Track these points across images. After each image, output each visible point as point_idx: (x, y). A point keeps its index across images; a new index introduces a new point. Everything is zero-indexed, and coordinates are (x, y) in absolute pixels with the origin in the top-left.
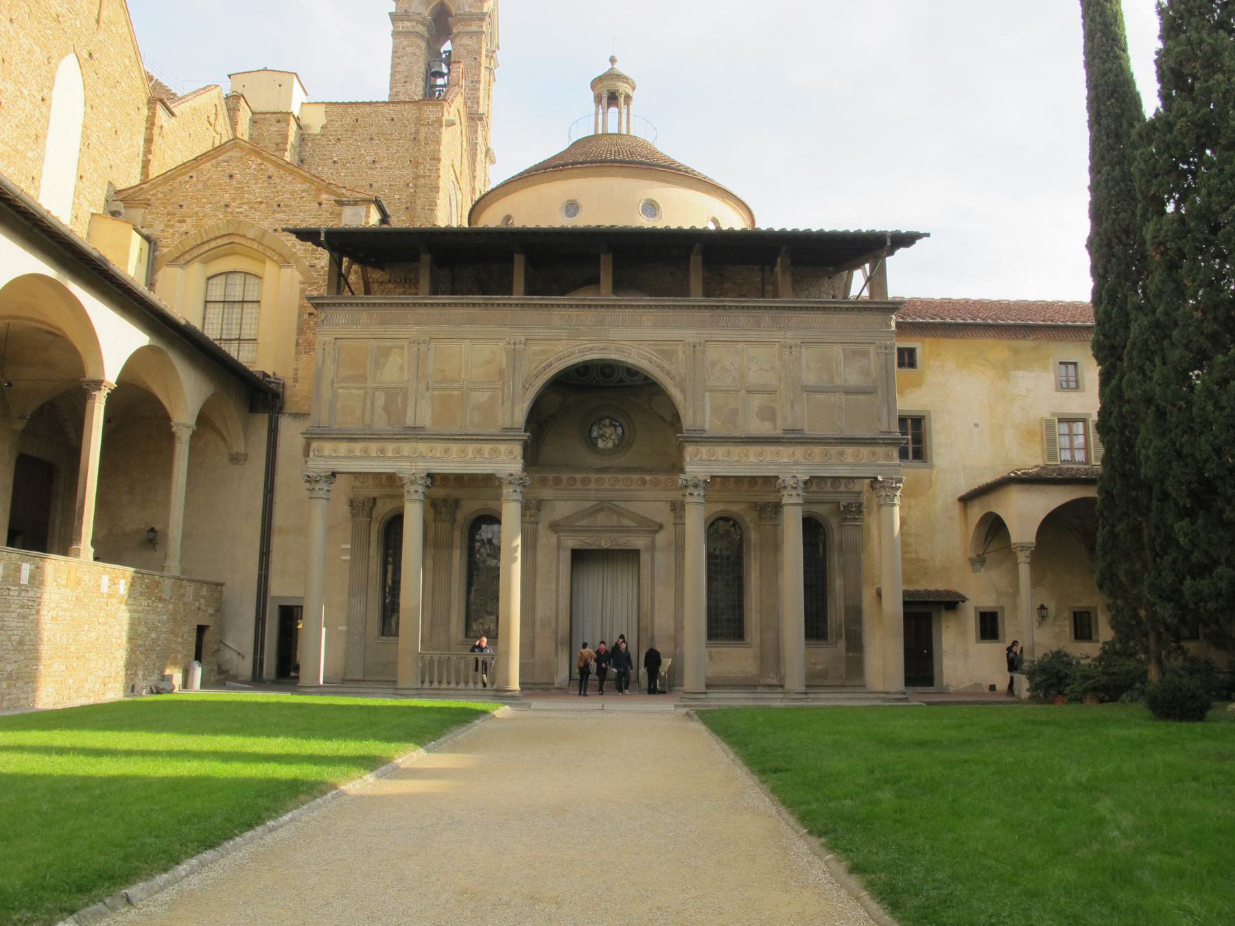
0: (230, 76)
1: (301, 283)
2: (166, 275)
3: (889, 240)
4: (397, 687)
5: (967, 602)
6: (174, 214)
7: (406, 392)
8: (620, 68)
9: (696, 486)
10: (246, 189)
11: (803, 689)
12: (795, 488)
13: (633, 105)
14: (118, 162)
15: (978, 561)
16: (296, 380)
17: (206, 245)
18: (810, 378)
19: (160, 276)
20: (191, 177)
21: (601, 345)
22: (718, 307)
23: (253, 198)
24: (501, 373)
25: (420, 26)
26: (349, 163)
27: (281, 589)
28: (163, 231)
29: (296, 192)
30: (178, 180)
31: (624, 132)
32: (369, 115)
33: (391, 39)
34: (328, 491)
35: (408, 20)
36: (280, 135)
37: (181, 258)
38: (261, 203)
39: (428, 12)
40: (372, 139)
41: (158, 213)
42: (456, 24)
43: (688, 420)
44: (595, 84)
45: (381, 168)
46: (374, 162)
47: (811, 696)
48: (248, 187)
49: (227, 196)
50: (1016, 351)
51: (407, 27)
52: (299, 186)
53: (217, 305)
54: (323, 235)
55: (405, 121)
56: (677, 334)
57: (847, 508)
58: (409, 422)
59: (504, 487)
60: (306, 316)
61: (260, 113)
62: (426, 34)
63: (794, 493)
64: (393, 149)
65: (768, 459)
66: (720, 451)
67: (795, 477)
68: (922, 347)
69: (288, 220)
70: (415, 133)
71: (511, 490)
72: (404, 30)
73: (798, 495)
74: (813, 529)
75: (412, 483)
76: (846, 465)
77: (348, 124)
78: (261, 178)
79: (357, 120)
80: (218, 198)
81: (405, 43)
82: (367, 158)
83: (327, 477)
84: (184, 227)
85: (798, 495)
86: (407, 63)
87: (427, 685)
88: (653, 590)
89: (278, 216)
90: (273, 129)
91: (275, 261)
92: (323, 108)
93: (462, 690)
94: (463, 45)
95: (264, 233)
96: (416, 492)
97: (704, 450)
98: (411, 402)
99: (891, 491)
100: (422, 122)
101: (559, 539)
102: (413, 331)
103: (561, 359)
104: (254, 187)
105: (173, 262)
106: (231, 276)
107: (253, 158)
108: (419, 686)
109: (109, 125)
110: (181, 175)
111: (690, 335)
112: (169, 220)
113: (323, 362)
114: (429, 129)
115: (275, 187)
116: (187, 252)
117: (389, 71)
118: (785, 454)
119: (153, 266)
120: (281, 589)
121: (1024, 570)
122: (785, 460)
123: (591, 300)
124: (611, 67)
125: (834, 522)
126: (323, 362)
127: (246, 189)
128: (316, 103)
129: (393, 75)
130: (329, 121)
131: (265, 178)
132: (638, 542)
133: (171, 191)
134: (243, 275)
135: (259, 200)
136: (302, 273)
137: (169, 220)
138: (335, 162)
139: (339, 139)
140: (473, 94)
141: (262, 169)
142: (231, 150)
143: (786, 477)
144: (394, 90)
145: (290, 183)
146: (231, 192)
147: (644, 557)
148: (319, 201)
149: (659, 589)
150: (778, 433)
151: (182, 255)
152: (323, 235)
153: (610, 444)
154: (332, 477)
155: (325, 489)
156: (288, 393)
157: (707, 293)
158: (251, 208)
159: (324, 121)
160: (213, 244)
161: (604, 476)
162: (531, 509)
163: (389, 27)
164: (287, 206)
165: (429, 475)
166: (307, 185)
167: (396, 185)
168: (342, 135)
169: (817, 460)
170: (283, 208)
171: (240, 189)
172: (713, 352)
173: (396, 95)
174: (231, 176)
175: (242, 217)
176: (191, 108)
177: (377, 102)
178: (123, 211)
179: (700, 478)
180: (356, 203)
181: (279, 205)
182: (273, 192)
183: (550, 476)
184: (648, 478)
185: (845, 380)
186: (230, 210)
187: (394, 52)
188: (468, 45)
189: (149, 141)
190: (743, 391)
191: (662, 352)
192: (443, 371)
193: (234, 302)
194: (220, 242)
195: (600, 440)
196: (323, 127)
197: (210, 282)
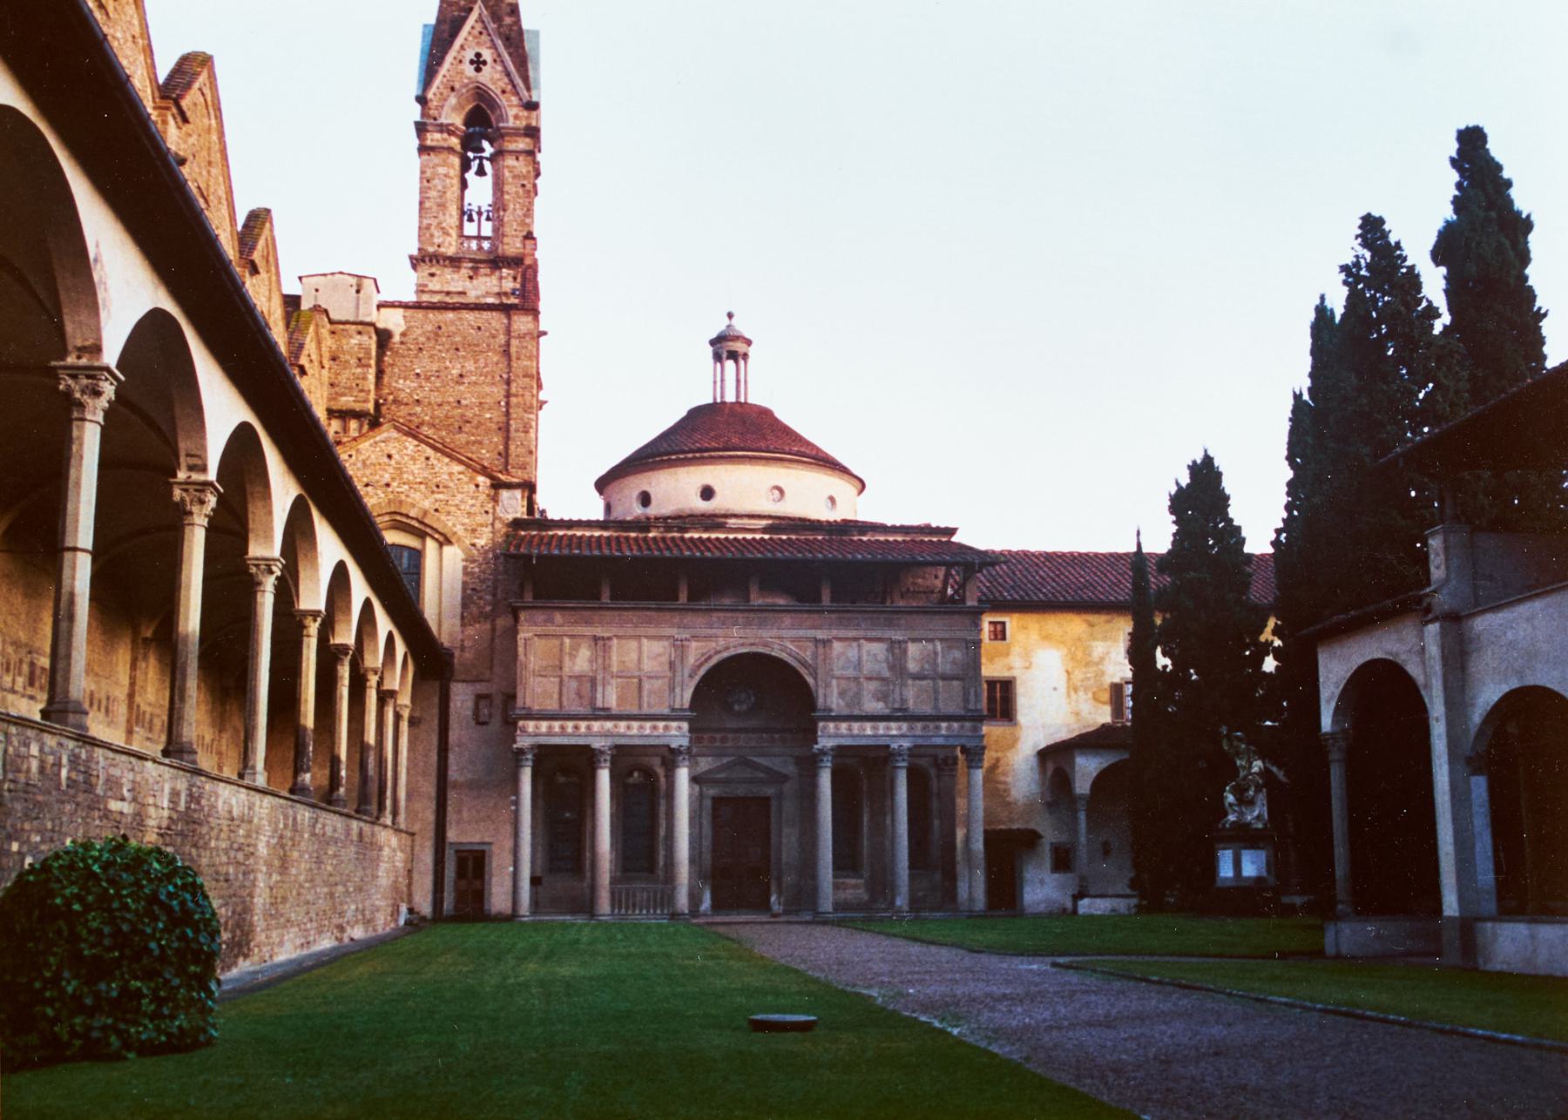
0: (300, 278)
1: (466, 560)
5: (1043, 840)
13: (750, 361)
15: (1051, 806)
16: (463, 648)
20: (350, 456)
24: (672, 665)
31: (742, 400)
32: (452, 322)
38: (421, 483)
40: (457, 349)
43: (820, 701)
44: (713, 343)
46: (461, 376)
49: (387, 476)
50: (1091, 625)
51: (438, 140)
56: (811, 633)
57: (945, 760)
58: (599, 704)
60: (469, 592)
62: (458, 148)
63: (900, 758)
64: (482, 363)
73: (903, 760)
74: (917, 779)
79: (440, 328)
80: (378, 477)
82: (454, 372)
87: (616, 911)
88: (780, 830)
91: (437, 540)
92: (400, 311)
94: (508, 167)
95: (425, 513)
96: (605, 760)
97: (831, 725)
98: (600, 689)
101: (701, 788)
102: (599, 631)
104: (413, 467)
107: (410, 439)
111: (821, 634)
118: (894, 728)
121: (1082, 816)
122: (894, 732)
125: (933, 772)
126: (525, 655)
131: (423, 459)
132: (769, 791)
135: (419, 480)
136: (463, 551)
138: (418, 374)
139: (420, 349)
141: (419, 451)
145: (447, 464)
146: (392, 471)
147: (774, 804)
149: (786, 830)
150: (887, 711)
153: (744, 707)
159: (403, 328)
163: (416, 142)
164: (445, 487)
166: (461, 468)
170: (441, 489)
171: (399, 470)
175: (403, 497)
180: (509, 486)
181: (438, 486)
184: (777, 736)
186: (390, 489)
187: (423, 172)
188: (514, 167)
191: (797, 647)
192: (624, 662)
196: (403, 334)
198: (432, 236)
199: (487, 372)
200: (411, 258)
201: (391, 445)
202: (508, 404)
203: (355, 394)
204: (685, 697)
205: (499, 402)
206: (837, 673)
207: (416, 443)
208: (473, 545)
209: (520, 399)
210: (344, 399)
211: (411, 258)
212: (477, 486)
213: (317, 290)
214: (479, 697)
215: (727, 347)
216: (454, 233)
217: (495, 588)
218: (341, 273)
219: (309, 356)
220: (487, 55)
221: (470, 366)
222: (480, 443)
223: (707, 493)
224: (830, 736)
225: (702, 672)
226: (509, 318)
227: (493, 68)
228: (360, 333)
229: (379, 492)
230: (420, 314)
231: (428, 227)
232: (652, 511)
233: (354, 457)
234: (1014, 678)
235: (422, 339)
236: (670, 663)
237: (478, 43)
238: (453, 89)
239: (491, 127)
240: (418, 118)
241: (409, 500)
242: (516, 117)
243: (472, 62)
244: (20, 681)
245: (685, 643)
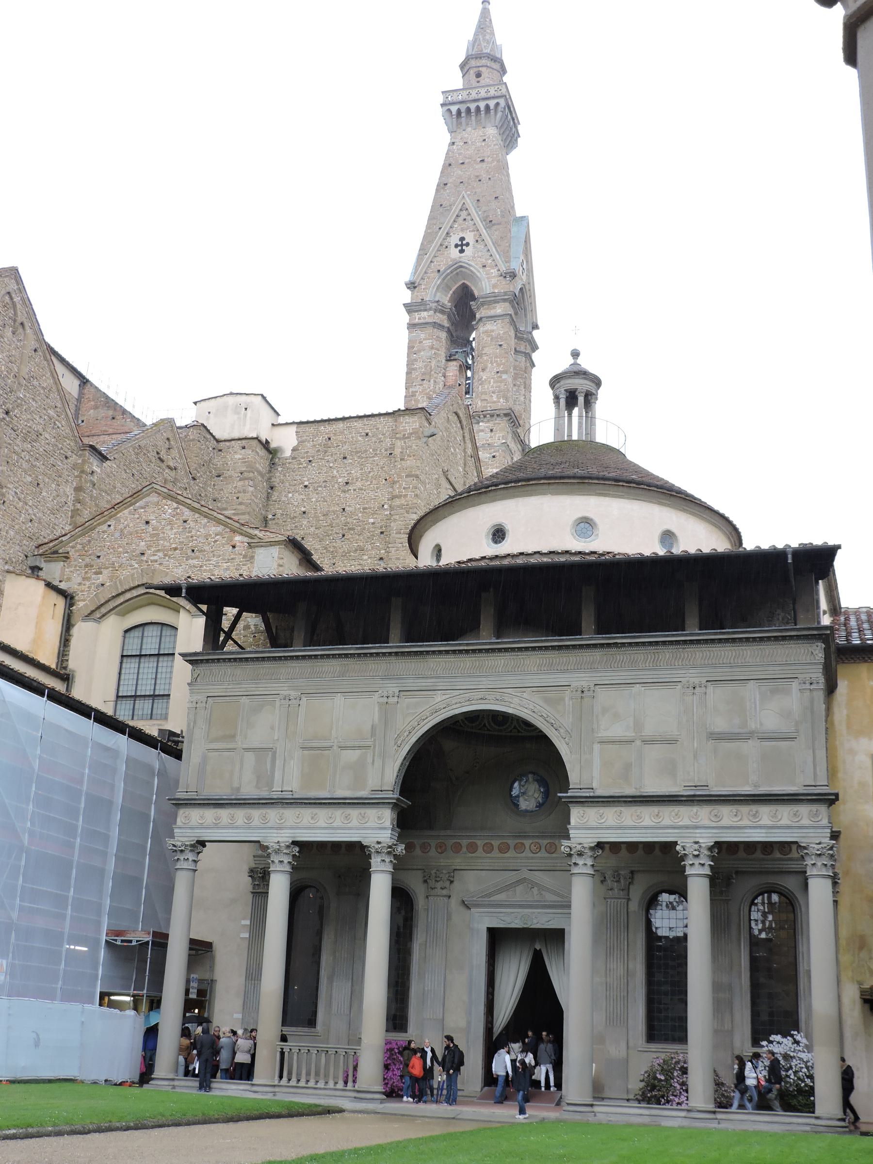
0: (195, 403)
2: (81, 630)
3: (790, 556)
4: (253, 1082)
6: (92, 566)
7: (275, 752)
8: (585, 363)
9: (580, 854)
10: (162, 535)
11: (711, 1107)
12: (697, 856)
14: (40, 515)
17: (121, 596)
18: (720, 724)
19: (75, 631)
20: (109, 526)
21: (480, 695)
22: (609, 645)
23: (168, 544)
25: (438, 314)
26: (321, 486)
28: (80, 584)
29: (210, 535)
30: (97, 530)
32: (342, 433)
33: (407, 331)
34: (195, 861)
35: (425, 310)
36: (245, 462)
37: (97, 612)
38: (176, 549)
39: (448, 298)
40: (345, 458)
41: (76, 566)
42: (478, 308)
43: (574, 776)
45: (355, 490)
46: (347, 483)
47: (719, 1116)
48: (164, 533)
49: (143, 544)
51: (424, 318)
52: (214, 528)
53: (133, 660)
54: (184, 591)
55: (380, 436)
56: (562, 679)
59: (373, 857)
61: (225, 441)
62: (446, 324)
63: (697, 862)
65: (667, 822)
66: (610, 815)
67: (696, 843)
69: (201, 566)
70: (390, 448)
71: (379, 860)
72: (422, 321)
75: (277, 851)
76: (761, 827)
77: (320, 445)
78: (176, 523)
79: (329, 439)
81: (423, 336)
82: (340, 480)
83: (192, 846)
84: (101, 579)
85: (703, 865)
86: (424, 358)
89: (190, 561)
90: (238, 456)
91: (189, 611)
92: (294, 428)
93: (320, 1089)
94: (486, 332)
98: (279, 763)
99: (818, 859)
100: (398, 436)
103: (436, 712)
105: (89, 616)
106: (147, 628)
107: (169, 502)
108: (276, 1083)
109: (29, 479)
110: (99, 525)
111: (580, 679)
112: (86, 573)
113: (195, 722)
114: (405, 443)
115: (190, 532)
116: (102, 605)
117: (405, 369)
118: (685, 815)
123: (467, 645)
124: (572, 361)
126: (195, 722)
127: (162, 535)
128: (287, 424)
130: (300, 443)
131: (180, 522)
133: (89, 541)
134: (160, 627)
135: (174, 546)
137: (86, 573)
138: (306, 486)
139: (310, 461)
140: (499, 387)
141: (177, 514)
142: (148, 495)
143: (686, 843)
144: (411, 390)
145: (205, 526)
148: (233, 544)
151: (99, 608)
152: (184, 591)
154: (200, 848)
155: (191, 859)
158: (165, 555)
159: (295, 443)
160: (128, 596)
161: (524, 841)
163: (406, 318)
165: (295, 843)
166: (220, 528)
167: (370, 508)
168: (313, 457)
169: (725, 822)
172: (604, 696)
173: (412, 396)
174: (147, 523)
176: (134, 448)
177: (350, 418)
178: (43, 565)
179: (585, 845)
181: (193, 551)
182: (188, 537)
183: (464, 842)
185: (761, 724)
186: (144, 558)
187: (410, 347)
188: (493, 331)
190: (638, 743)
193: (150, 655)
194: (135, 593)
195: (521, 799)
196: (294, 450)
197: (128, 635)
198: (417, 401)
199: (372, 477)
201: (150, 510)
202: (390, 507)
203: (235, 507)
205: (383, 506)
206: (604, 734)
207: (175, 505)
209: (403, 501)
212: (234, 547)
213: (209, 413)
218: (231, 394)
219: (162, 461)
220: (470, 238)
221: (356, 472)
223: (499, 534)
225: (414, 739)
226: (396, 421)
227: (474, 247)
228: (244, 448)
229: (133, 563)
230: (311, 429)
231: (413, 394)
233: (112, 527)
235: (312, 452)
236: (373, 726)
237: (462, 230)
238: (439, 271)
239: (473, 298)
240: (409, 301)
242: (494, 286)
243: (456, 246)
245: (391, 700)
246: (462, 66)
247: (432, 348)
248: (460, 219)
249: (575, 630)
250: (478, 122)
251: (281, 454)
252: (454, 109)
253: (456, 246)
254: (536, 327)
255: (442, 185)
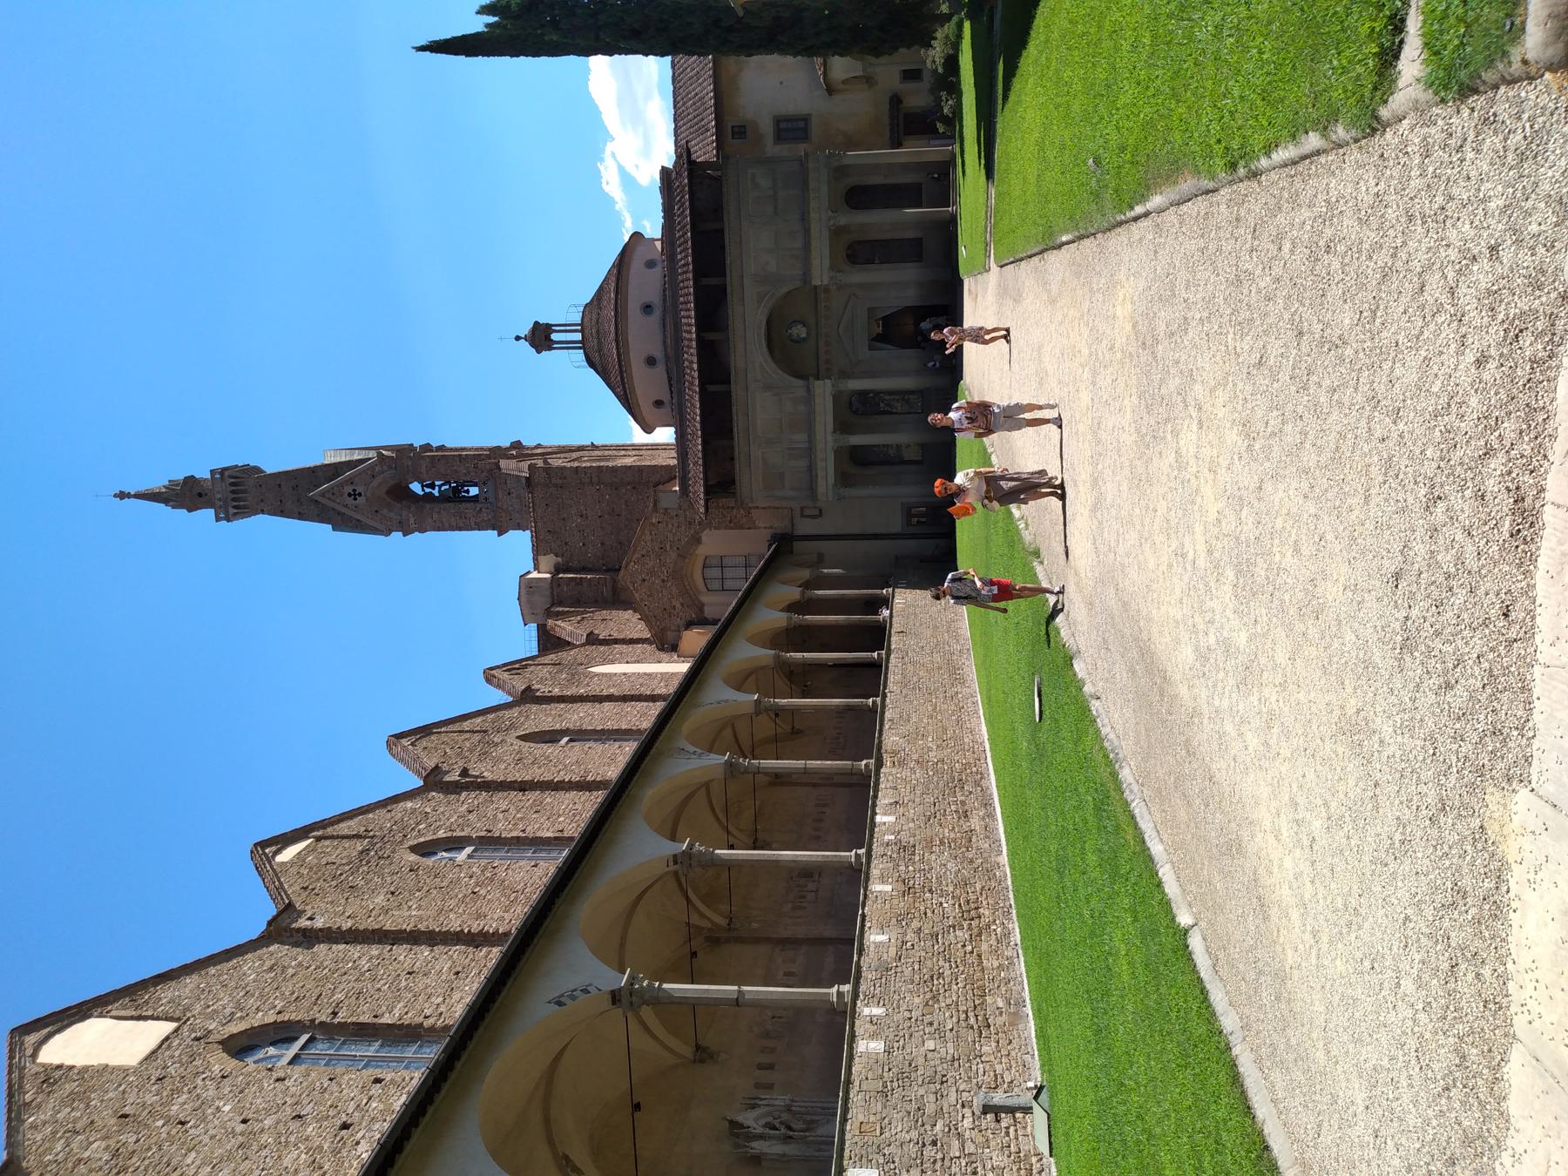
2: (709, 613)
16: (771, 527)
27: (896, 525)
66: (816, 262)
68: (730, 122)
84: (678, 605)
92: (541, 558)
94: (427, 471)
95: (679, 555)
111: (746, 281)
119: (703, 622)
120: (896, 525)
129: (460, 529)
153: (804, 329)
156: (778, 531)
157: (725, 275)
162: (845, 375)
164: (661, 543)
165: (834, 432)
166: (647, 532)
174: (644, 580)
189: (616, 641)
200: (500, 535)
204: (800, 382)
208: (700, 524)
210: (605, 594)
211: (500, 535)
214: (802, 516)
215: (541, 337)
216: (479, 506)
217: (728, 508)
220: (349, 489)
222: (626, 501)
224: (821, 274)
225: (780, 372)
227: (356, 485)
232: (666, 397)
234: (774, 117)
241: (672, 566)
244: (811, 886)
246: (190, 510)
247: (439, 513)
248: (332, 497)
249: (723, 289)
250: (244, 492)
251: (559, 563)
252: (232, 511)
253: (355, 499)
254: (412, 445)
255: (301, 516)
